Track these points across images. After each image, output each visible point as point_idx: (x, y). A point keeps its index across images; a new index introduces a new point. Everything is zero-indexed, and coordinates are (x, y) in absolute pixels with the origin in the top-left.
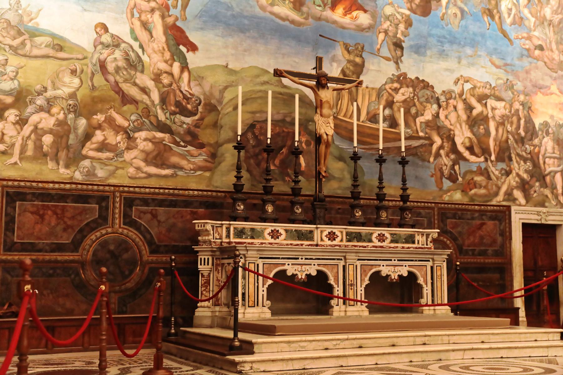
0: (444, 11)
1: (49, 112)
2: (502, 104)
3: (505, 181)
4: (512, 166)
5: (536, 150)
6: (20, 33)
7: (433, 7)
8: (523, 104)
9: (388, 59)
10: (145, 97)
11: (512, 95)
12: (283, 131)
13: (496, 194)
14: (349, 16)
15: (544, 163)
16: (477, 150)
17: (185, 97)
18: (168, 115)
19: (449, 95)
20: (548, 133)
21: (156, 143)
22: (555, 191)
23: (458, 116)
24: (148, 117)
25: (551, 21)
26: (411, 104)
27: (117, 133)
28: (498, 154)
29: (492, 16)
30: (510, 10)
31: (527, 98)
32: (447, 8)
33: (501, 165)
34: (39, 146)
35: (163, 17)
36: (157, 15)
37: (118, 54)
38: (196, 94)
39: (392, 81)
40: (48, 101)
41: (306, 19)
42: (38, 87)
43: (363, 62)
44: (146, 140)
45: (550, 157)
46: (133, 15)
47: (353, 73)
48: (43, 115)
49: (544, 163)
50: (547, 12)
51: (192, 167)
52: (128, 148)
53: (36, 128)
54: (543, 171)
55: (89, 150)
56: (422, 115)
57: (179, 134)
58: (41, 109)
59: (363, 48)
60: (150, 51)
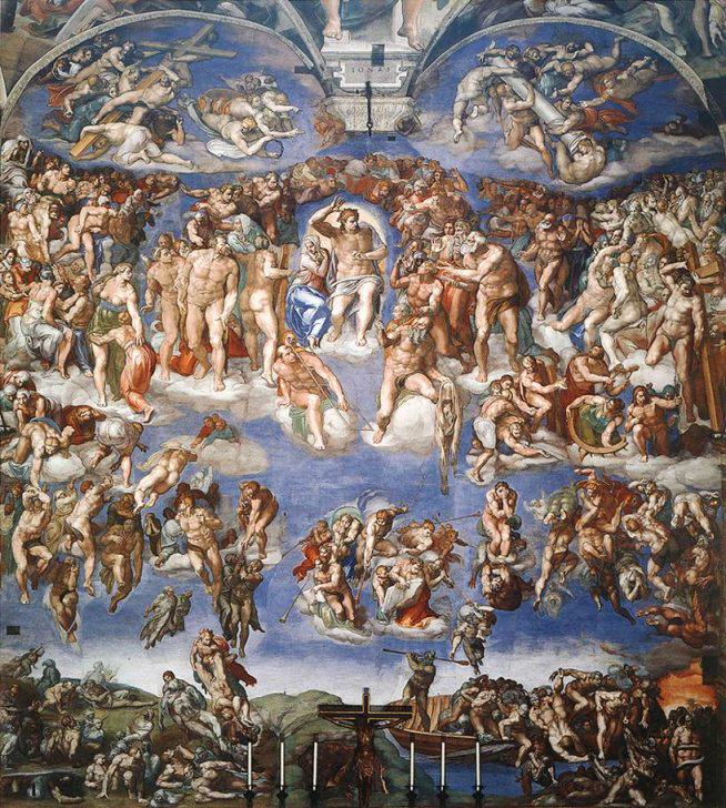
1: (128, 753)
2: (618, 694)
6: (103, 690)
9: (465, 663)
13: (606, 795)
15: (676, 755)
19: (541, 692)
23: (555, 713)
25: (694, 585)
27: (184, 765)
29: (605, 595)
30: (634, 582)
32: (542, 595)
34: (121, 779)
35: (223, 657)
37: (184, 696)
39: (469, 685)
40: (126, 743)
41: (367, 636)
42: (119, 733)
45: (685, 749)
48: (124, 756)
52: (195, 778)
53: (118, 768)
56: (507, 717)
58: (122, 751)
59: (433, 656)
60: (212, 689)
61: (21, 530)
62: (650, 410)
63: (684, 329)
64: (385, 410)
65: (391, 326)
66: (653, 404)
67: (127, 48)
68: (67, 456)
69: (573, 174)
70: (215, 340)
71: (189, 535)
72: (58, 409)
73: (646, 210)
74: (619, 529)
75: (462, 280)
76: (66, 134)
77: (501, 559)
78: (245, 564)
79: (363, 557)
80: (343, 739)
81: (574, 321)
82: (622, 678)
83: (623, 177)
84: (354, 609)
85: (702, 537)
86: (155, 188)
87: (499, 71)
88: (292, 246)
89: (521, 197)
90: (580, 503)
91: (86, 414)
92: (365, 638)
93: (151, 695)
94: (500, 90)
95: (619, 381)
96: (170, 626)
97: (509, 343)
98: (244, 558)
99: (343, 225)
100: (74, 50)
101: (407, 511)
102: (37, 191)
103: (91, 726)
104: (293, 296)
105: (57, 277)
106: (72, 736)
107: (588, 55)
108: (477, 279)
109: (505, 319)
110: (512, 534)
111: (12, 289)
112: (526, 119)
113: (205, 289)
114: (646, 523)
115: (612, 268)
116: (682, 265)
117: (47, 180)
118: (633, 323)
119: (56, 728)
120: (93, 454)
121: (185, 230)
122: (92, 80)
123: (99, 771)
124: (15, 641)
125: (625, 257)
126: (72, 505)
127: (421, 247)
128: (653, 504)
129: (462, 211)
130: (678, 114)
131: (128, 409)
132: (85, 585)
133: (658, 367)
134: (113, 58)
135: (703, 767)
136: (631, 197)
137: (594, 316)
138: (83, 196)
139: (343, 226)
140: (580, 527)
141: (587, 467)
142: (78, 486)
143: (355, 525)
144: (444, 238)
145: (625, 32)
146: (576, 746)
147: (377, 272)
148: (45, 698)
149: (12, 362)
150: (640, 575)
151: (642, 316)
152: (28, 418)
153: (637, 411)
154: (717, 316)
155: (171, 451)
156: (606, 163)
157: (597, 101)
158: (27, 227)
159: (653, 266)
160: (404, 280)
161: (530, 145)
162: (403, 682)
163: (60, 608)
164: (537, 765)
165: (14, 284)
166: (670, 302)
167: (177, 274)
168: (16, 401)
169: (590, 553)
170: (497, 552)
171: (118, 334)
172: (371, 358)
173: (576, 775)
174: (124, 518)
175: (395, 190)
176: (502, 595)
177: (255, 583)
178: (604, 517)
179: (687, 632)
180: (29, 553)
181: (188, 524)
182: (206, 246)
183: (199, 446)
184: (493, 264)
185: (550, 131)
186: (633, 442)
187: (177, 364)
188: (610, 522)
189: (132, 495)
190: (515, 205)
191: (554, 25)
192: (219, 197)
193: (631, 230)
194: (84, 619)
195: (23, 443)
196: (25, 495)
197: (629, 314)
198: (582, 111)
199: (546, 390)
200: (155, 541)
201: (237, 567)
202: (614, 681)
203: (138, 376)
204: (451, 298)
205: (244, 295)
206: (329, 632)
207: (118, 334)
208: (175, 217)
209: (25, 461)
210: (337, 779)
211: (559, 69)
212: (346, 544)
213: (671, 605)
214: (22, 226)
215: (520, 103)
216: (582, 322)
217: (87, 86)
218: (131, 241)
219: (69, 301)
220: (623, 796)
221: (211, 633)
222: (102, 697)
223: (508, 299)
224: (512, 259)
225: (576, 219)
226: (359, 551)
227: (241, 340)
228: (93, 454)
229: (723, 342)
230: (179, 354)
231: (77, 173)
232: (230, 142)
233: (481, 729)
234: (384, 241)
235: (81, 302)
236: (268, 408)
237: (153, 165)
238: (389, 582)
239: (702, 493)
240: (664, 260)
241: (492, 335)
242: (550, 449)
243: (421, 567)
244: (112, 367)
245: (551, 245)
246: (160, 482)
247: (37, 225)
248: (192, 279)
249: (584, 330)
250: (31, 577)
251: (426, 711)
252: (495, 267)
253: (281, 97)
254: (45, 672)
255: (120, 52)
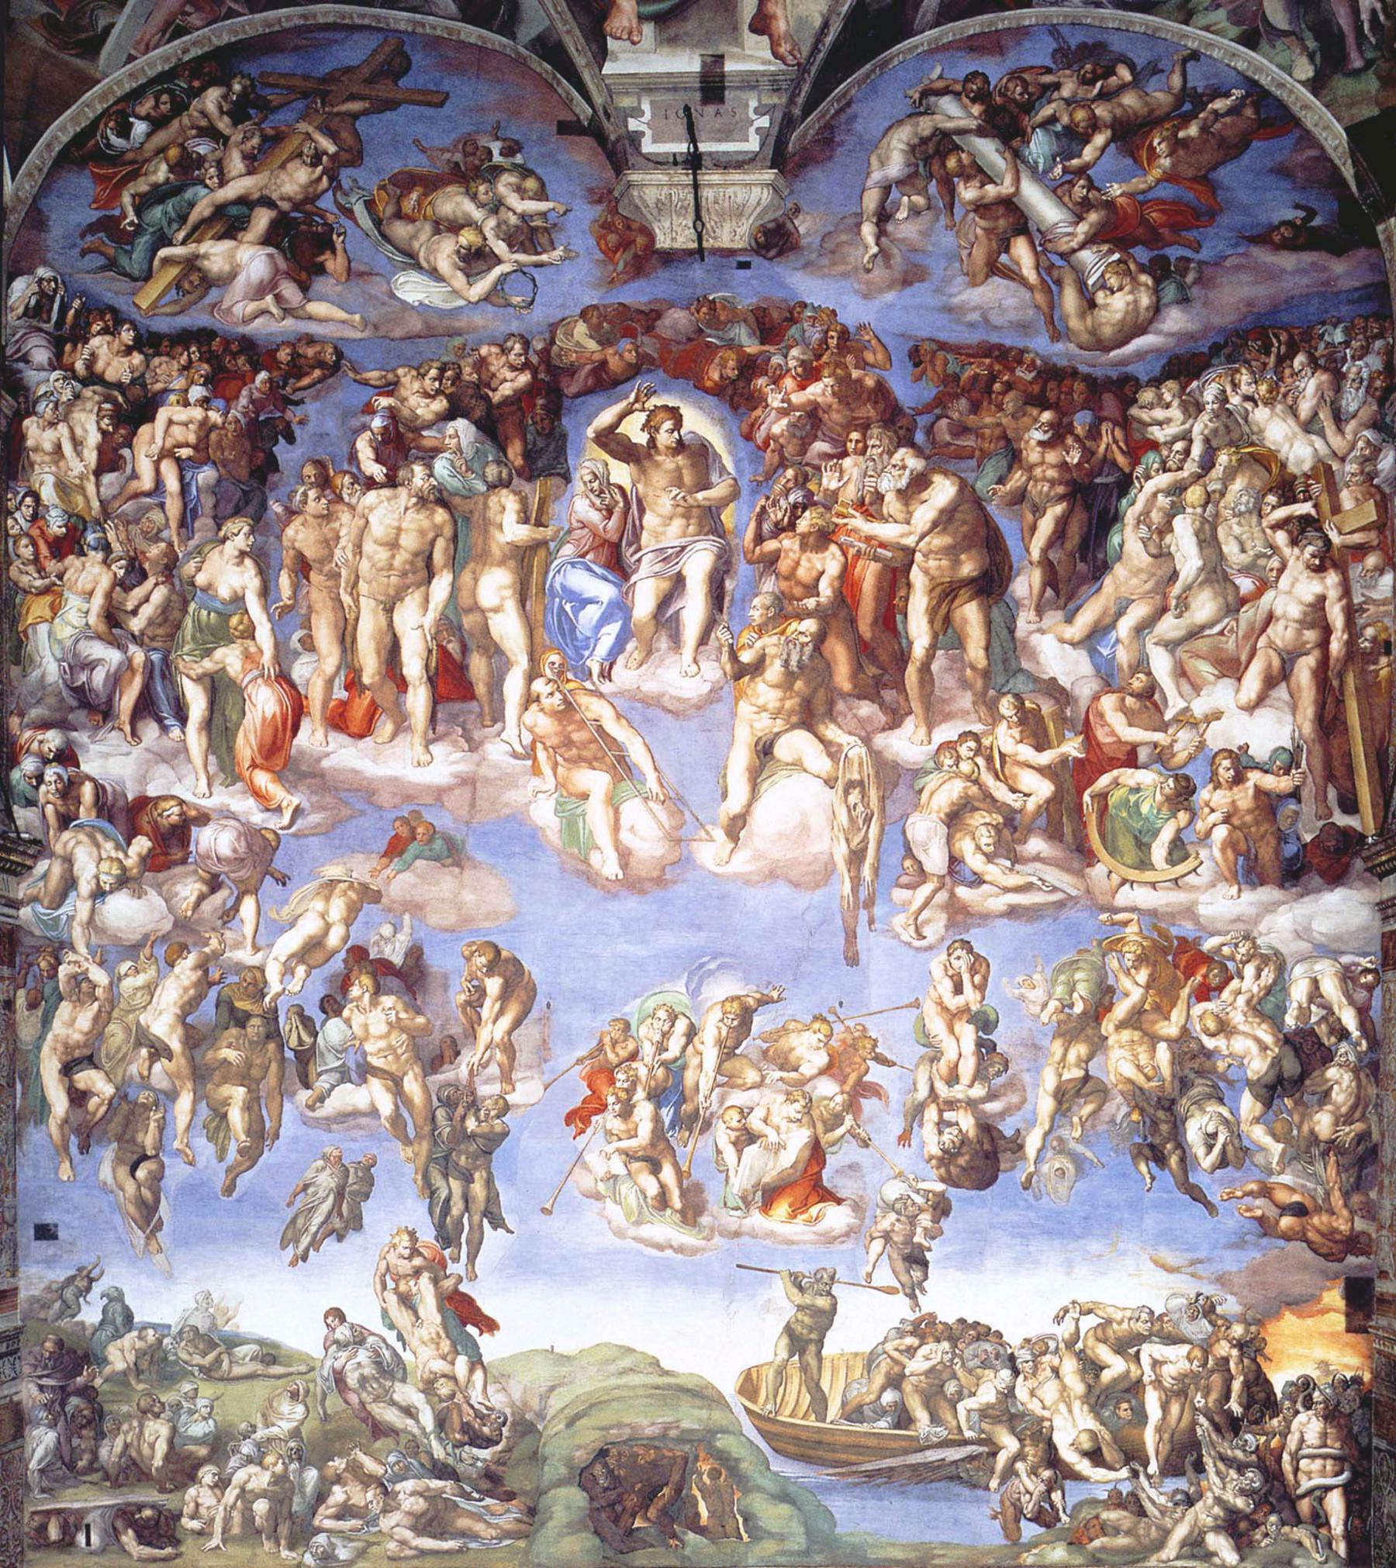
0: (1032, 1169)
1: (260, 1464)
2: (1185, 1348)
3: (1184, 1515)
4: (1204, 1483)
5: (1274, 1443)
6: (212, 1345)
7: (1002, 1166)
8: (1241, 1345)
9: (890, 1291)
10: (410, 1422)
11: (1210, 1329)
12: (664, 1457)
13: (1160, 1545)
14: (801, 1217)
15: (1296, 1470)
16: (1108, 1454)
17: (478, 1415)
18: (449, 1448)
19: (1039, 1347)
20: (1308, 1404)
21: (432, 1497)
22: (1323, 1531)
24: (416, 1455)
26: (945, 1376)
28: (1167, 1460)
29: (1160, 1160)
30: (1214, 1136)
31: (1253, 1329)
33: (1172, 1484)
35: (435, 1281)
36: (425, 1279)
37: (363, 1356)
38: (498, 1406)
39: (901, 1333)
40: (258, 1445)
42: (243, 1426)
43: (834, 1306)
44: (413, 1494)
46: (384, 1287)
47: (811, 1330)
48: (253, 1469)
49: (1296, 1470)
50: (1323, 1123)
51: (494, 1533)
52: (385, 1511)
54: (1291, 1490)
55: (323, 1519)
57: (470, 1480)
58: (250, 1460)
59: (832, 1278)
60: (414, 1342)
61: (56, 1039)
62: (1244, 797)
63: (1311, 636)
64: (735, 803)
65: (744, 639)
66: (1250, 784)
67: (237, 87)
68: (139, 894)
69: (1093, 332)
70: (413, 666)
71: (369, 1047)
72: (121, 803)
73: (1235, 400)
74: (1185, 1031)
75: (883, 545)
76: (123, 261)
77: (959, 1092)
78: (474, 1105)
79: (697, 1089)
80: (664, 1436)
81: (1097, 623)
82: (1193, 1318)
83: (1191, 337)
84: (680, 1186)
85: (1344, 1047)
86: (296, 369)
87: (950, 125)
88: (558, 480)
89: (993, 378)
90: (1111, 981)
91: (172, 813)
92: (702, 1243)
93: (300, 1353)
94: (952, 163)
95: (1184, 741)
96: (337, 1223)
97: (973, 668)
98: (473, 1093)
99: (652, 441)
100: (136, 95)
101: (779, 999)
102: (75, 377)
103: (192, 1412)
104: (559, 579)
105: (116, 546)
106: (157, 1431)
107: (1123, 87)
108: (910, 541)
109: (965, 621)
110: (980, 1044)
111: (31, 569)
112: (1002, 223)
113: (391, 567)
114: (1237, 1018)
115: (1169, 517)
116: (1305, 508)
117: (93, 354)
118: (1212, 625)
119: (129, 1416)
120: (188, 889)
121: (353, 457)
122: (173, 153)
123: (207, 1498)
124: (51, 1252)
125: (1194, 494)
126: (150, 989)
127: (802, 481)
128: (1250, 982)
129: (881, 406)
130: (1297, 207)
131: (251, 802)
132: (176, 1144)
133: (1257, 712)
134: (211, 107)
135: (1347, 1489)
136: (1210, 374)
137: (1138, 612)
138: (159, 386)
139: (652, 441)
140: (1111, 1028)
141: (1125, 910)
142: (160, 951)
143: (681, 1025)
144: (847, 462)
145: (1193, 36)
146: (1105, 1450)
147: (718, 531)
148: (104, 1361)
149: (34, 713)
150: (1226, 1122)
151: (1225, 616)
152: (65, 821)
153: (1221, 798)
154: (1372, 609)
155: (332, 883)
156: (1157, 309)
157: (1138, 183)
158: (58, 448)
159: (1250, 512)
160: (771, 545)
161: (1012, 274)
162: (775, 1326)
163: (130, 1187)
164: (1031, 1487)
165: (36, 560)
166: (1284, 582)
167: (338, 538)
168: (43, 788)
169: (1130, 1081)
170: (953, 1079)
171: (229, 658)
172: (713, 696)
173: (1107, 1504)
174: (248, 1016)
175: (750, 367)
176: (962, 1161)
177: (495, 1139)
178: (1157, 1008)
179: (1318, 1231)
180: (71, 1081)
181: (366, 1027)
182: (392, 482)
183: (388, 871)
184: (942, 512)
185: (1049, 246)
186: (1213, 859)
187: (342, 715)
188: (1168, 1018)
189: (261, 969)
190: (981, 394)
191: (1053, 30)
192: (416, 386)
193: (1207, 441)
194: (174, 1210)
195: (58, 870)
196: (63, 971)
197: (1204, 607)
198: (1110, 205)
199: (1046, 758)
200: (305, 1057)
201: (460, 1110)
202: (1176, 1324)
203: (268, 739)
204: (862, 580)
205: (466, 577)
206: (633, 1231)
207: (229, 658)
208: (331, 425)
209: (59, 906)
210: (652, 1513)
211: (1065, 120)
212: (664, 1064)
213: (1287, 1179)
214: (48, 446)
215: (990, 189)
216: (1113, 625)
217: (164, 167)
218: (252, 474)
219: (138, 593)
220: (1195, 1546)
221: (412, 1234)
222: (211, 1357)
223: (970, 582)
224: (978, 503)
225: (1099, 420)
226: (689, 1077)
227: (462, 668)
228: (188, 889)
229: (1384, 660)
230: (343, 695)
231: (149, 343)
232: (434, 274)
233: (921, 1415)
234: (728, 462)
235: (159, 595)
236: (515, 797)
237: (289, 323)
238: (746, 1137)
239: (1346, 959)
240: (1272, 499)
241: (940, 653)
242: (1054, 876)
243: (808, 1108)
244: (218, 720)
245: (1051, 473)
246: (312, 950)
247: (77, 443)
248: (368, 547)
249: (1118, 641)
250: (78, 1131)
251: (818, 1384)
252: (945, 519)
253: (531, 184)
254: (104, 1311)
255: (225, 97)
